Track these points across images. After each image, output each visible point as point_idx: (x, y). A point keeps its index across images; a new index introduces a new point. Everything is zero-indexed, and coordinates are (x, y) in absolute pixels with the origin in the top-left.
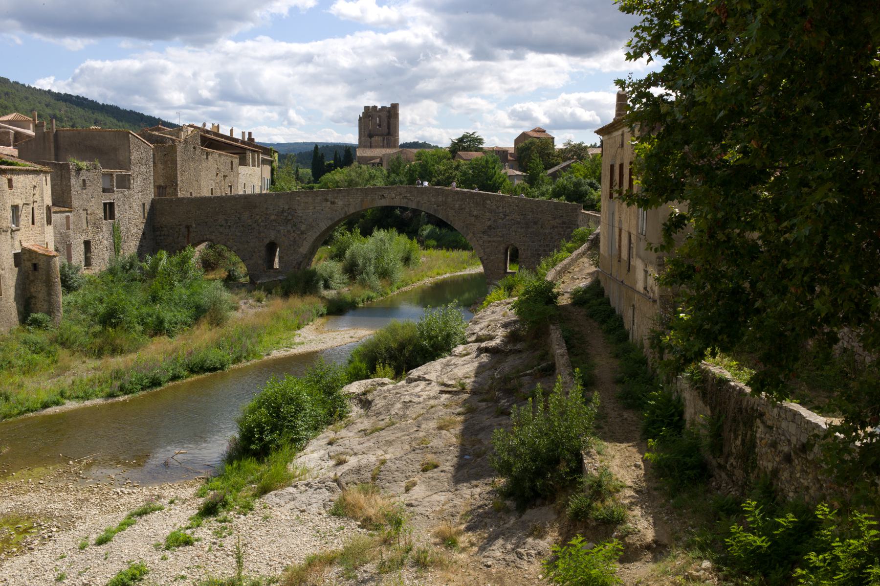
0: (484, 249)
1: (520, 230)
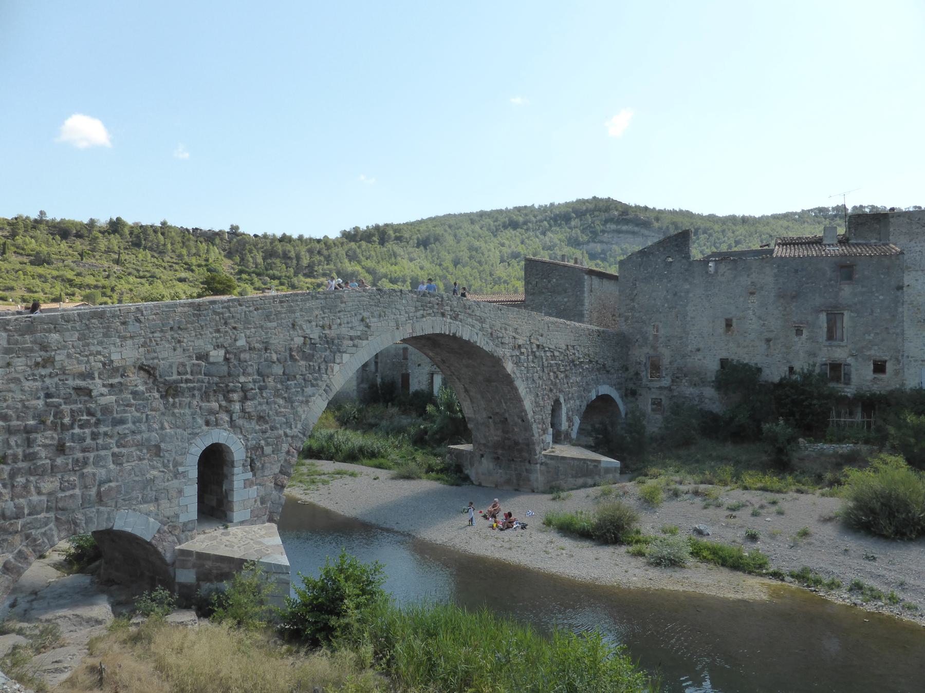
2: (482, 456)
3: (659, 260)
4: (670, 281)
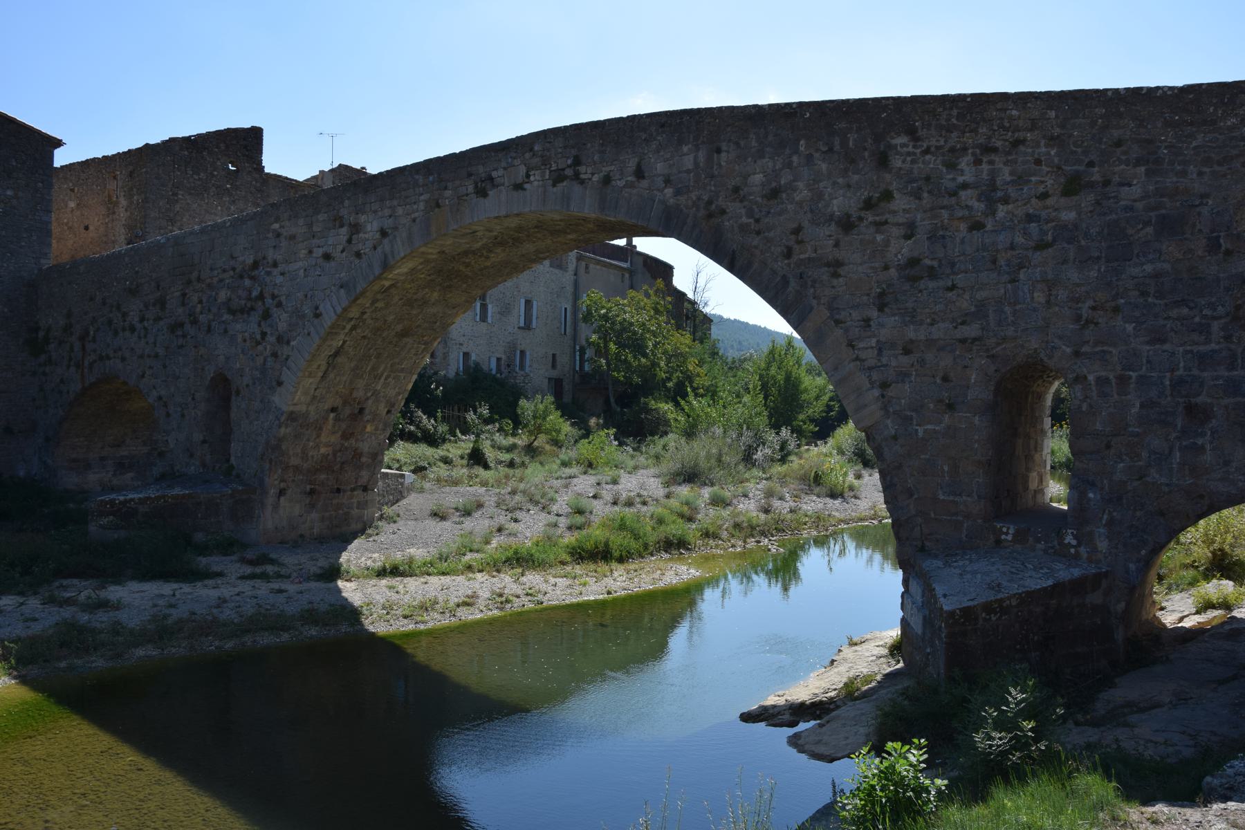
0: (884, 385)
1: (1073, 275)
2: (282, 492)
3: (219, 163)
4: (234, 202)
